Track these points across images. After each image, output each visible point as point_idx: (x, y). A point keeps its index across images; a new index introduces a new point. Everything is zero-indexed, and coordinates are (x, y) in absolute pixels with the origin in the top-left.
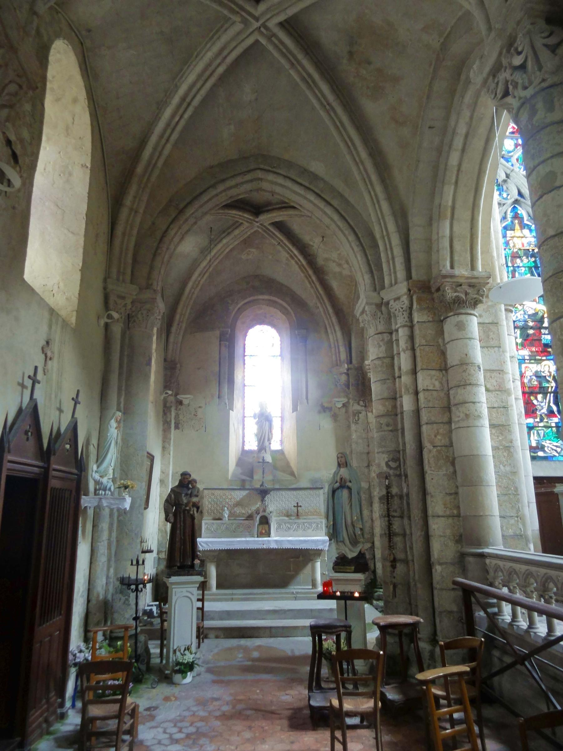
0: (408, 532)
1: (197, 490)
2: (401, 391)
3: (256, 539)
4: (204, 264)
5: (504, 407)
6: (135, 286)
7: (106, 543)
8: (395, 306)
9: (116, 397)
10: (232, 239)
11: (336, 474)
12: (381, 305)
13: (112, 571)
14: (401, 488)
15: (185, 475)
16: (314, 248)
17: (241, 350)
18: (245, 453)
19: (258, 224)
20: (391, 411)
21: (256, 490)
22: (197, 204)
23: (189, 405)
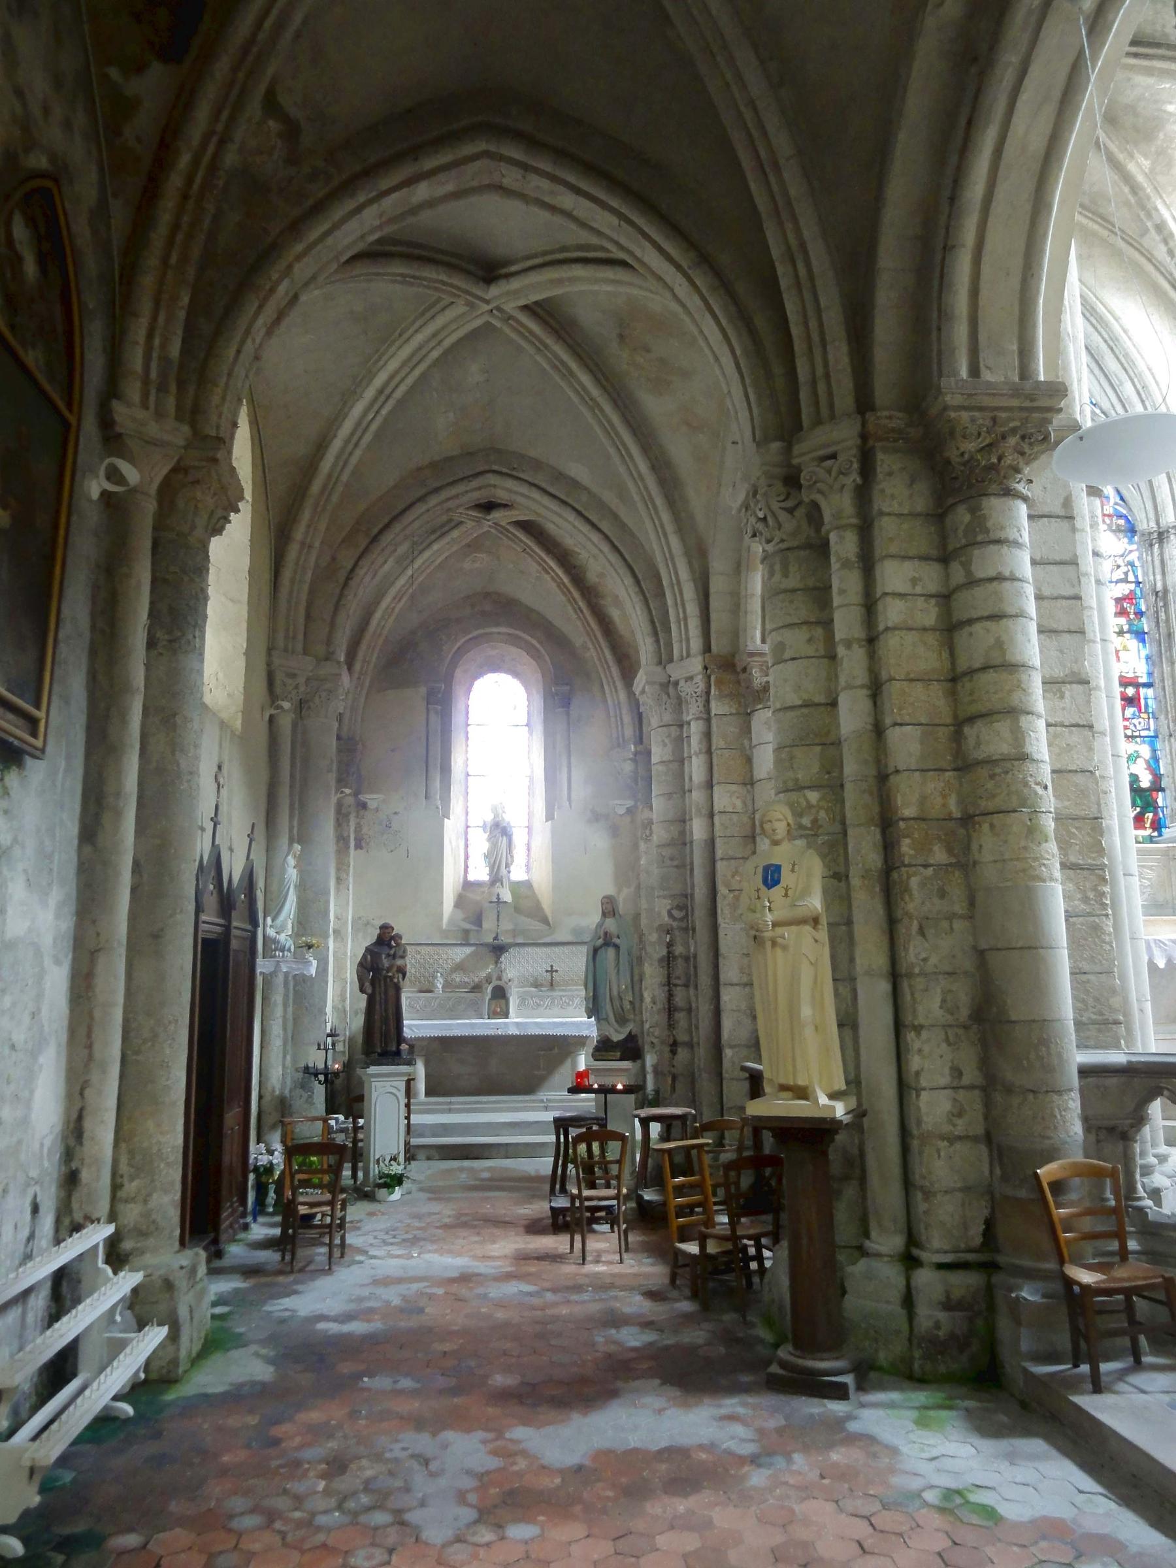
0: (694, 1005)
2: (690, 811)
6: (308, 658)
7: (280, 1020)
8: (686, 689)
9: (287, 817)
11: (600, 925)
12: (668, 685)
13: (288, 1058)
14: (686, 945)
15: (385, 928)
18: (467, 885)
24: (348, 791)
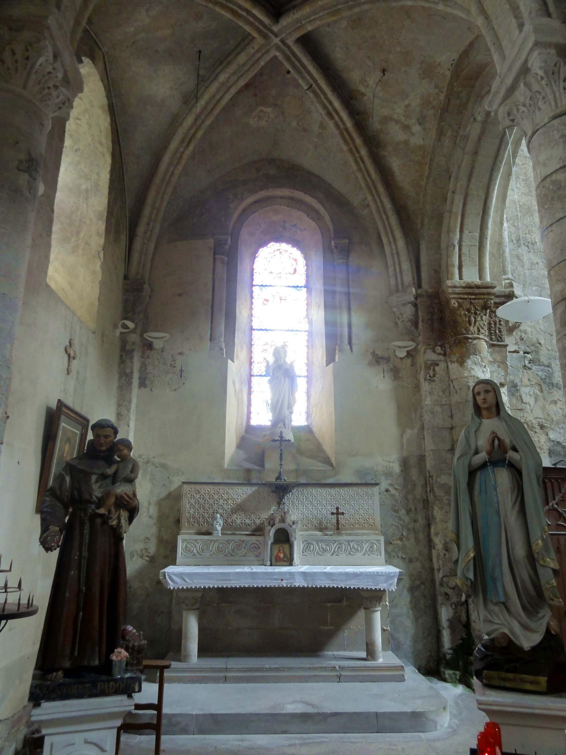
1: (130, 466)
3: (270, 569)
4: (190, 120)
10: (234, 73)
16: (365, 98)
18: (250, 429)
19: (277, 40)
21: (269, 485)
23: (163, 350)
24: (131, 325)
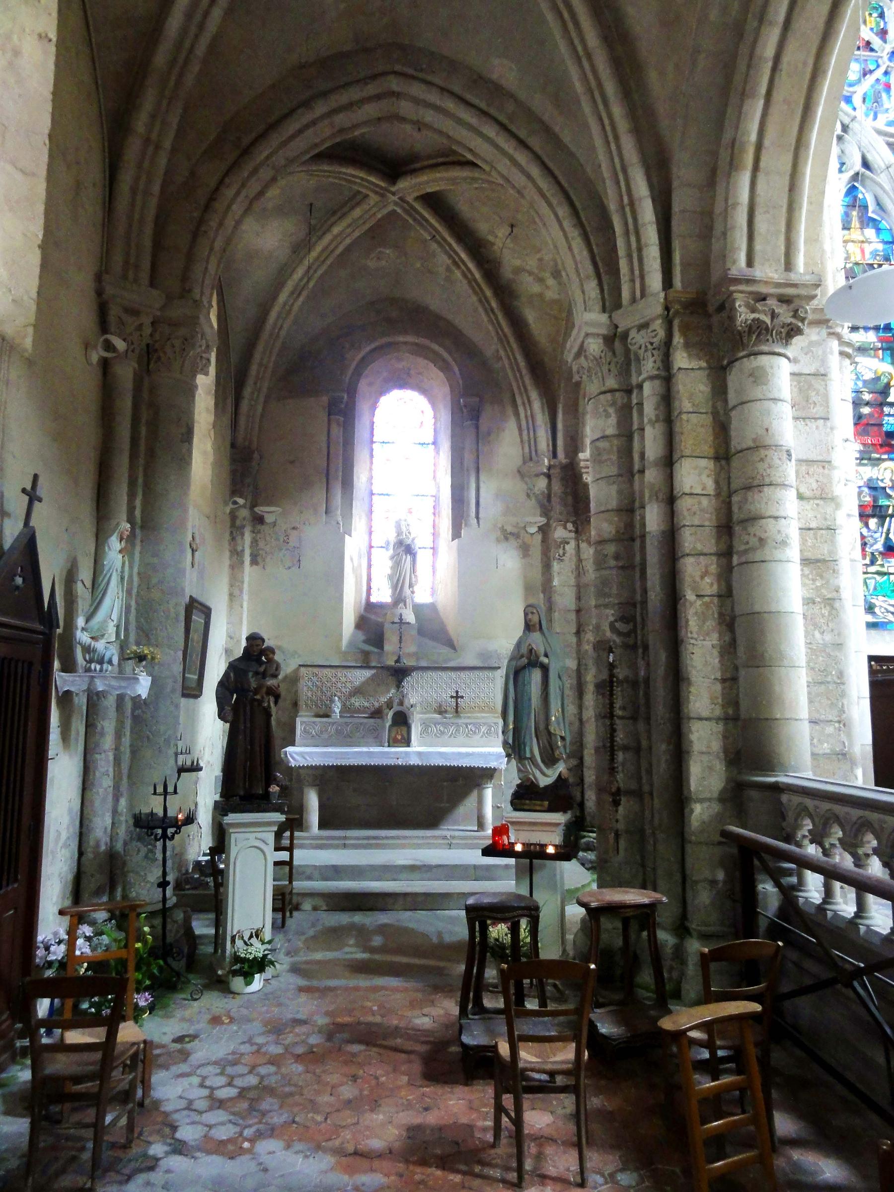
0: (644, 743)
2: (642, 497)
3: (387, 749)
4: (300, 272)
5: (829, 529)
6: (155, 292)
8: (638, 339)
9: (125, 498)
10: (349, 226)
13: (123, 802)
14: (634, 666)
16: (496, 247)
17: (366, 435)
18: (370, 606)
19: (395, 198)
20: (623, 533)
22: (275, 139)
23: (274, 524)
24: (241, 501)
